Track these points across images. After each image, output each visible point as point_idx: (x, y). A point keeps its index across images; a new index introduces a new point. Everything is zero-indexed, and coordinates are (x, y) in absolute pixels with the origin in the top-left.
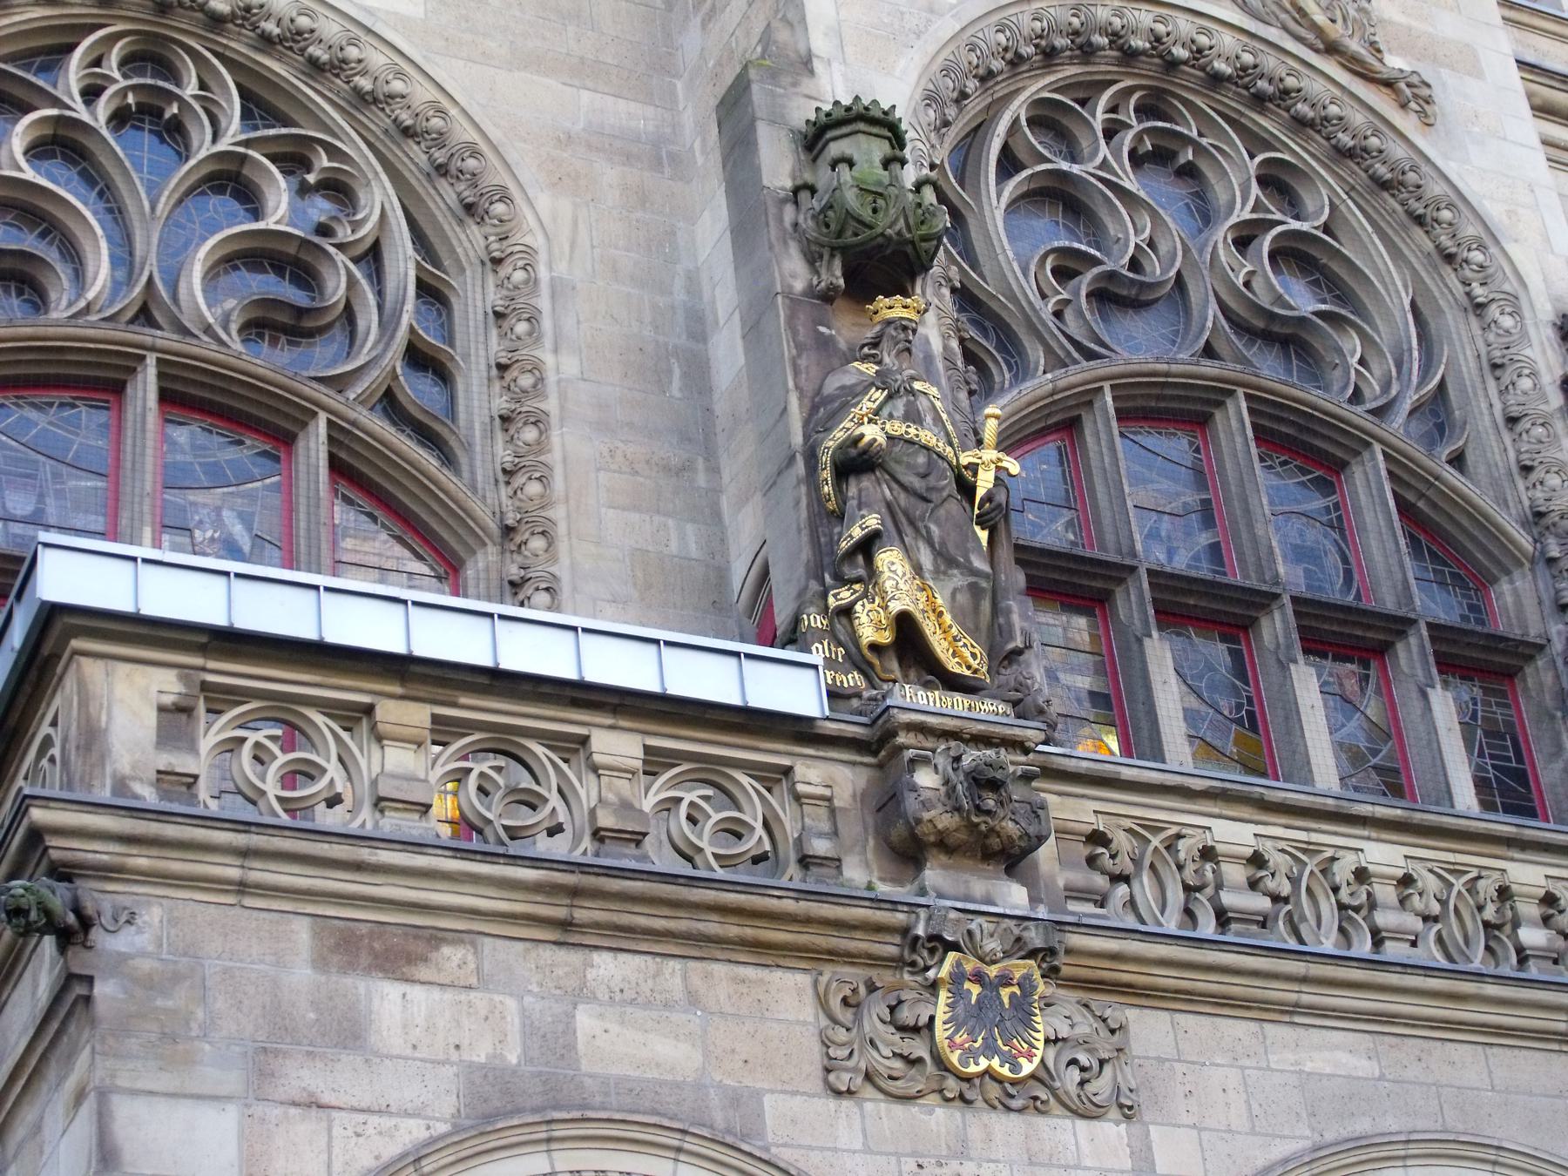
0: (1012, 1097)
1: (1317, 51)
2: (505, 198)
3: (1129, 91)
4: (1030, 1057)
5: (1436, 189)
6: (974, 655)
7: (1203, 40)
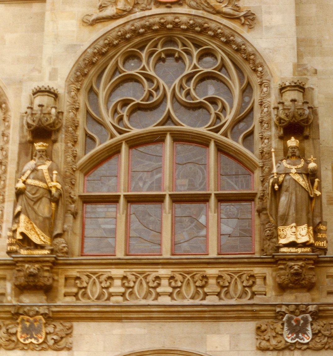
0: (37, 348)
1: (214, 14)
2: (5, 103)
3: (159, 40)
4: (41, 338)
5: (250, 49)
6: (44, 238)
7: (177, 20)
